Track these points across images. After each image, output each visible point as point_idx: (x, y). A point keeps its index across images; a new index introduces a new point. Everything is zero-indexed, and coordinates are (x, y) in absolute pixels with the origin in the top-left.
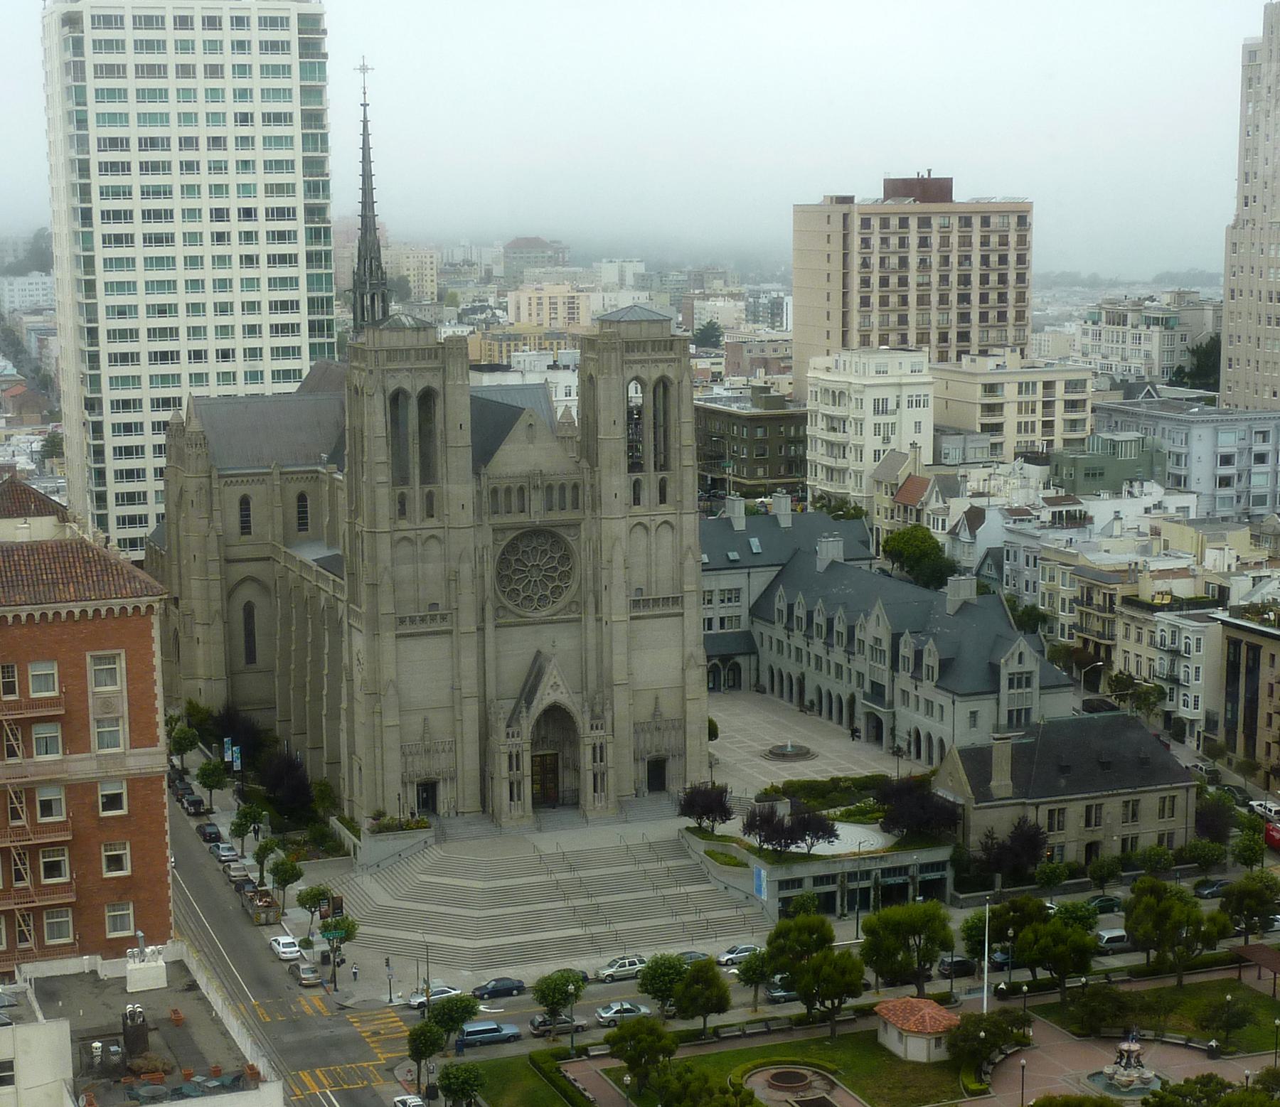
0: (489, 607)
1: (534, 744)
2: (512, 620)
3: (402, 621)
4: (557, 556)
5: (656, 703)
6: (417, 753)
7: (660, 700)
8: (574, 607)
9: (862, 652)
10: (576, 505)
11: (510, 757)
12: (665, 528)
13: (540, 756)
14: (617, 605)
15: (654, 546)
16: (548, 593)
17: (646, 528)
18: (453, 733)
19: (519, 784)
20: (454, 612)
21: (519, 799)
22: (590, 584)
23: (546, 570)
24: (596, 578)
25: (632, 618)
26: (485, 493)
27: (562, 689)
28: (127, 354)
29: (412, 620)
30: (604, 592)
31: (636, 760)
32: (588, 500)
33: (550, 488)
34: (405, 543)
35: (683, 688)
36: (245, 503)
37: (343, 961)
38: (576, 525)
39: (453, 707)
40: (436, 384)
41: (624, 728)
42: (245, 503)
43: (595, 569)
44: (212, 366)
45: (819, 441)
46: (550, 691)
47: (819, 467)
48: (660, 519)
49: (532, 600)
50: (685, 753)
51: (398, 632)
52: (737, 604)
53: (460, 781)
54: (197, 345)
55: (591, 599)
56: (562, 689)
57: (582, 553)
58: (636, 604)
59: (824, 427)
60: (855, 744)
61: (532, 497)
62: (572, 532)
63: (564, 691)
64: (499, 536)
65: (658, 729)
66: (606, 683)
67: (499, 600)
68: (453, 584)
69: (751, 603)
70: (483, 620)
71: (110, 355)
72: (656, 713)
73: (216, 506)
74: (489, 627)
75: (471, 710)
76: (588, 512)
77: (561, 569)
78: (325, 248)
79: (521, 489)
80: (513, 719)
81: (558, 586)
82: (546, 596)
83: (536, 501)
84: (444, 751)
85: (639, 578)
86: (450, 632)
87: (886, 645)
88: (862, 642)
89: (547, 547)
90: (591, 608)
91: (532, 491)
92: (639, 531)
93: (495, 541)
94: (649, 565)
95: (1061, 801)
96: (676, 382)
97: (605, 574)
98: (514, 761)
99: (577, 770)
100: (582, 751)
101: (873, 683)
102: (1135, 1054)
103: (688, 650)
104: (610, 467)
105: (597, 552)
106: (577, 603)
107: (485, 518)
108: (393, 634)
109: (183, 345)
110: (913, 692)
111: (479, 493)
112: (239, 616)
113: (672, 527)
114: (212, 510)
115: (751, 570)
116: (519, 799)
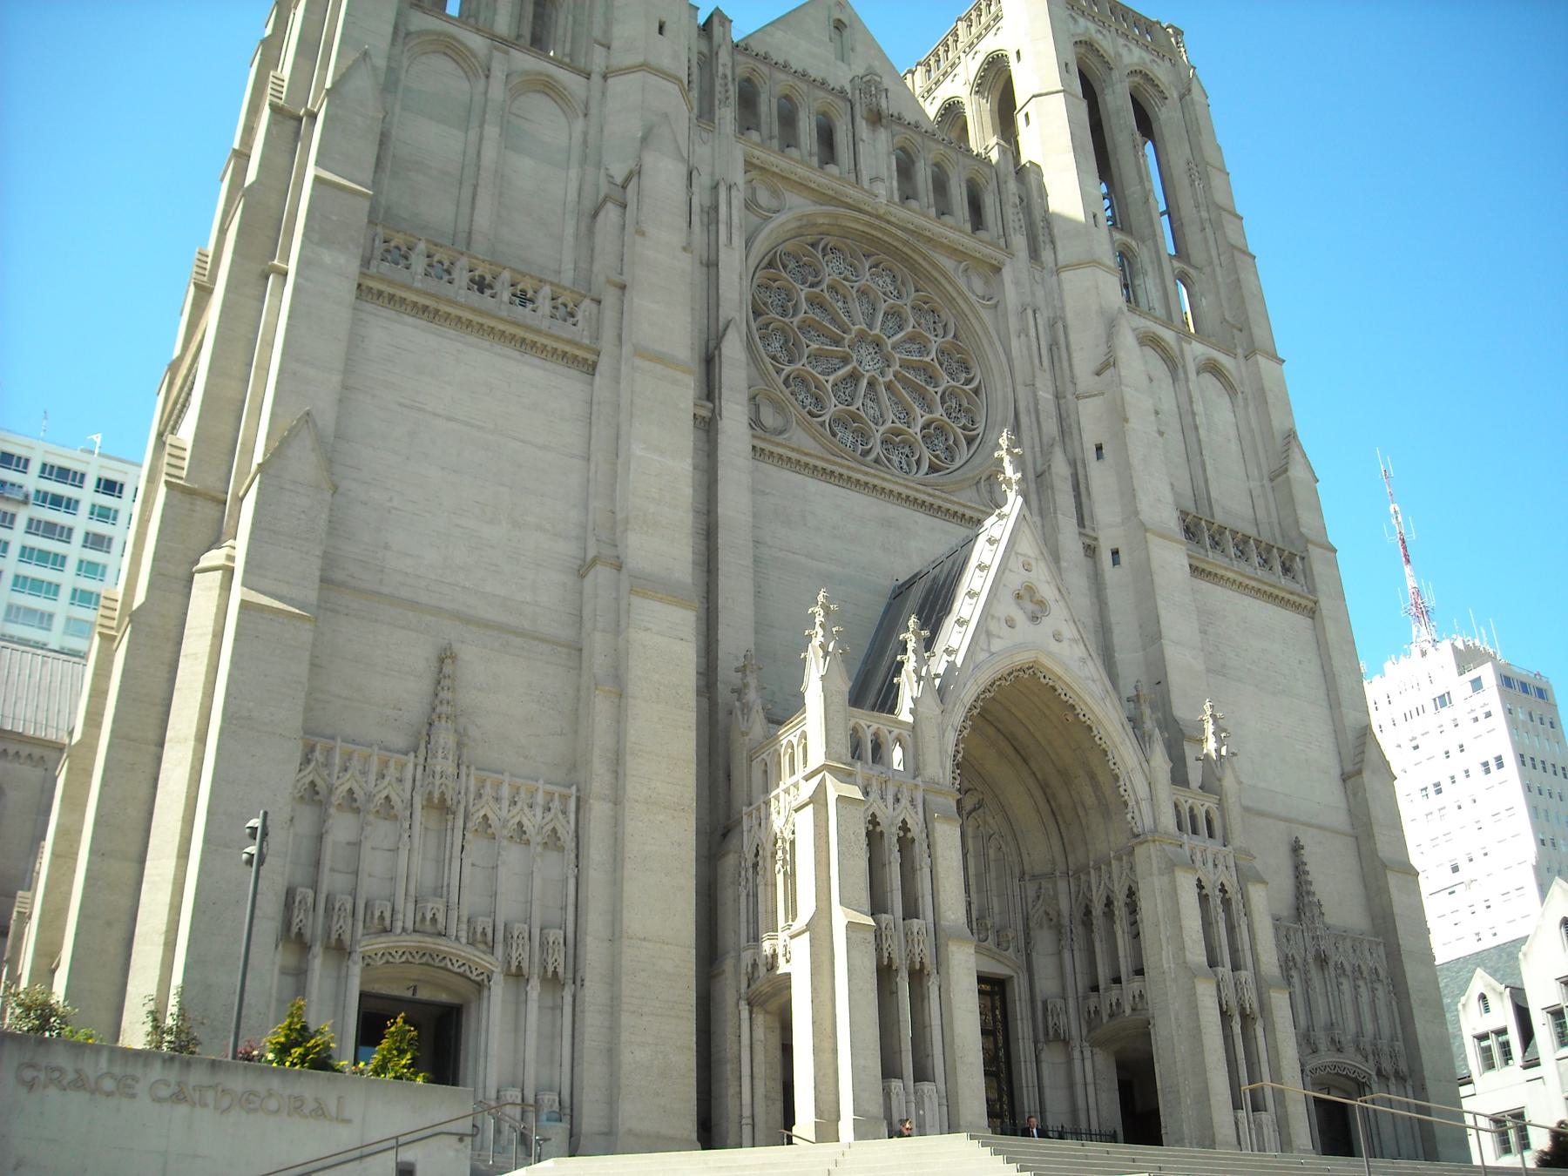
0: (733, 350)
7: (1307, 855)
15: (1198, 407)
17: (1172, 363)
20: (610, 298)
22: (1051, 427)
23: (905, 365)
27: (1057, 617)
39: (577, 650)
43: (1058, 396)
46: (1020, 617)
49: (863, 435)
53: (594, 992)
56: (1057, 617)
57: (1015, 343)
63: (1068, 631)
65: (1322, 960)
68: (611, 213)
76: (1019, 242)
77: (945, 381)
81: (940, 429)
91: (863, 128)
93: (750, 204)
113: (1229, 387)
116: (921, 1075)
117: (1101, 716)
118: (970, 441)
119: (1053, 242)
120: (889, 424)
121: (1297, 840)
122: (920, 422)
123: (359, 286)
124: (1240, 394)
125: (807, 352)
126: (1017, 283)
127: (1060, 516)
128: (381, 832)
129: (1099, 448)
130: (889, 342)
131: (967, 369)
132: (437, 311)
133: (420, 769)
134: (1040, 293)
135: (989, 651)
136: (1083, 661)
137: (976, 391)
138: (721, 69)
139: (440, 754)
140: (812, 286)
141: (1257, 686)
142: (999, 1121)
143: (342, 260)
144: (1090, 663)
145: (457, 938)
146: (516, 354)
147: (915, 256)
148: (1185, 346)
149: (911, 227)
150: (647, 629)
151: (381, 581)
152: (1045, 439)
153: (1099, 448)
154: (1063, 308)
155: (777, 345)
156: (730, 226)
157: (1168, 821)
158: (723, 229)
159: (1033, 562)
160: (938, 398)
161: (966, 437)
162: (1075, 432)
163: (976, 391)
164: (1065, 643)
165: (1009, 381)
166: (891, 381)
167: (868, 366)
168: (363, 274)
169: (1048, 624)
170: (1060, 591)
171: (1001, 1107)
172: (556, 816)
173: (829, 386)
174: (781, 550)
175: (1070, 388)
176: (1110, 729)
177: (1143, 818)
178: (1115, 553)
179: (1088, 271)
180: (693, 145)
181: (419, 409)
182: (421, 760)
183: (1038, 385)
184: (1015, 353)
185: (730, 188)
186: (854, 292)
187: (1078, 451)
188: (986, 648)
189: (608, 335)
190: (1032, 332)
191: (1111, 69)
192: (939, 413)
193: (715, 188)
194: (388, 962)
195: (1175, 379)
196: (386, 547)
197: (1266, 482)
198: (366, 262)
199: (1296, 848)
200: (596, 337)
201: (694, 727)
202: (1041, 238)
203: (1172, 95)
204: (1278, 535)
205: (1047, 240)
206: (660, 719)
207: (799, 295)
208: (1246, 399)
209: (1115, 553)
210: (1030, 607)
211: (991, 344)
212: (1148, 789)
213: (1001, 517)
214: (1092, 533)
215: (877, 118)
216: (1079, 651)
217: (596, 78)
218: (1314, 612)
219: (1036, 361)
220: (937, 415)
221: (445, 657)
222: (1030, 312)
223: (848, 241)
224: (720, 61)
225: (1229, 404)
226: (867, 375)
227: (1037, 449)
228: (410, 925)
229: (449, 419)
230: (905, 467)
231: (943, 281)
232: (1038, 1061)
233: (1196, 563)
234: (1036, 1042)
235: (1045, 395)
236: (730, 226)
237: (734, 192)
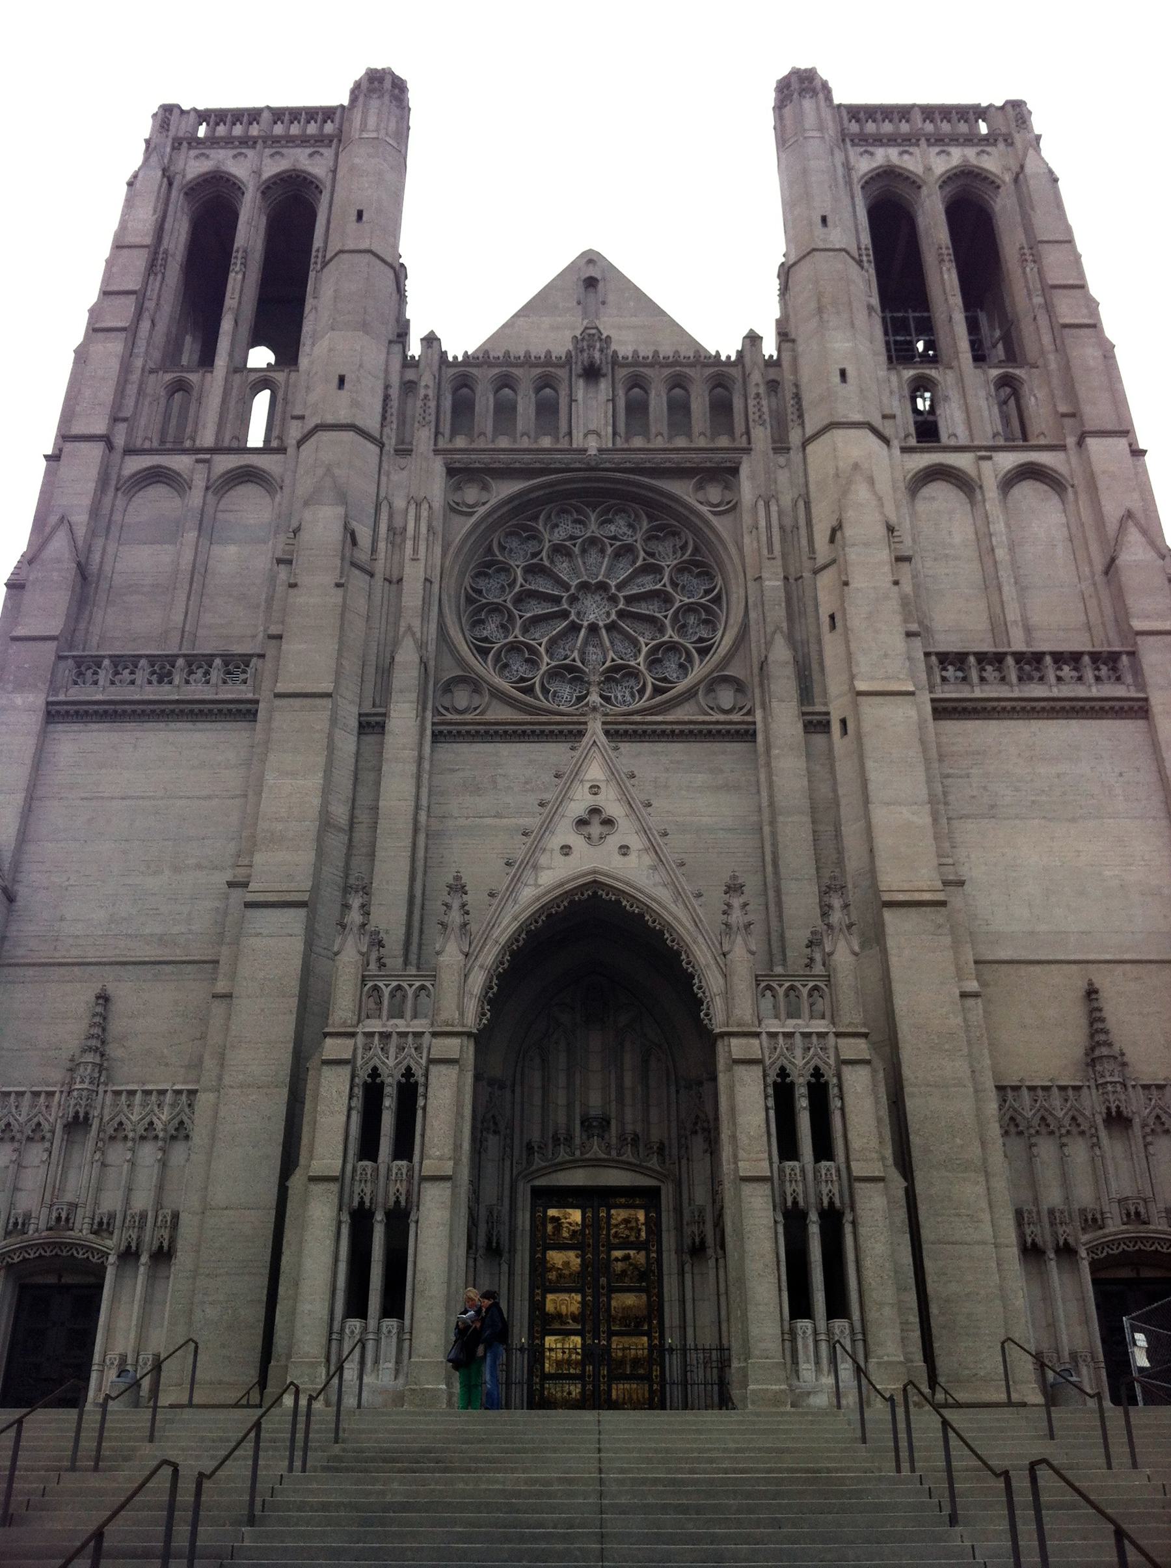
0: (407, 656)
2: (500, 713)
3: (86, 666)
4: (669, 562)
6: (36, 1134)
8: (726, 697)
11: (372, 1092)
12: (1027, 491)
18: (197, 1064)
22: (777, 614)
23: (629, 600)
25: (943, 710)
27: (626, 832)
29: (123, 663)
30: (827, 637)
31: (1031, 1252)
33: (637, 382)
34: (157, 493)
38: (726, 474)
40: (317, 167)
48: (1008, 461)
51: (62, 697)
55: (781, 653)
56: (626, 832)
57: (747, 540)
61: (580, 394)
62: (714, 493)
63: (636, 842)
64: (471, 494)
65: (1118, 1120)
67: (461, 662)
76: (761, 436)
81: (672, 647)
82: (634, 674)
84: (148, 1133)
86: (245, 712)
89: (637, 539)
90: (783, 684)
93: (453, 509)
94: (991, 585)
96: (1008, 178)
104: (820, 310)
106: (739, 686)
108: (36, 699)
117: (670, 919)
118: (703, 652)
119: (801, 416)
120: (608, 664)
121: (1091, 984)
122: (645, 650)
123: (48, 713)
124: (1070, 490)
125: (519, 622)
126: (752, 477)
127: (774, 704)
128: (36, 1154)
129: (832, 617)
130: (613, 583)
131: (712, 578)
132: (115, 712)
133: (65, 1094)
134: (783, 477)
135: (537, 886)
136: (654, 868)
137: (717, 600)
138: (422, 392)
139: (78, 1080)
140: (534, 555)
141: (1044, 818)
142: (645, 1339)
143: (31, 698)
144: (661, 868)
145: (81, 1231)
146: (189, 725)
147: (643, 492)
148: (981, 462)
149: (628, 465)
150: (258, 935)
151: (55, 949)
152: (769, 629)
153: (832, 617)
154: (807, 485)
155: (493, 626)
156: (416, 538)
158: (409, 544)
159: (603, 785)
160: (667, 622)
161: (699, 651)
162: (810, 610)
164: (633, 857)
165: (741, 580)
166: (613, 621)
167: (594, 611)
168: (48, 703)
169: (614, 841)
170: (631, 806)
171: (650, 1324)
172: (182, 1110)
173: (542, 650)
174: (467, 818)
175: (807, 564)
176: (681, 930)
178: (844, 722)
179: (828, 435)
180: (388, 475)
181: (97, 798)
182: (66, 1088)
183: (765, 575)
184: (747, 550)
185: (418, 505)
186: (576, 550)
187: (812, 629)
188: (531, 882)
189: (266, 685)
190: (762, 523)
191: (919, 187)
192: (670, 635)
194: (56, 1254)
195: (972, 503)
196: (62, 919)
197: (1099, 578)
198: (53, 688)
199: (1091, 993)
201: (295, 1010)
202: (790, 417)
203: (1004, 182)
204: (1112, 634)
205: (795, 417)
206: (262, 1010)
207: (516, 573)
208: (1076, 493)
209: (844, 722)
210: (595, 829)
211: (726, 549)
212: (721, 981)
213: (573, 749)
214: (823, 709)
215: (592, 373)
216: (648, 860)
217: (291, 451)
218: (1147, 711)
219: (765, 552)
220: (666, 638)
221: (104, 998)
222: (761, 503)
223: (573, 502)
224: (423, 384)
225: (1060, 506)
226: (585, 624)
227: (763, 641)
228: (42, 1226)
229: (123, 798)
230: (628, 698)
231: (673, 505)
232: (682, 1273)
233: (937, 704)
234: (679, 1251)
235: (773, 583)
236: (416, 538)
237: (425, 506)
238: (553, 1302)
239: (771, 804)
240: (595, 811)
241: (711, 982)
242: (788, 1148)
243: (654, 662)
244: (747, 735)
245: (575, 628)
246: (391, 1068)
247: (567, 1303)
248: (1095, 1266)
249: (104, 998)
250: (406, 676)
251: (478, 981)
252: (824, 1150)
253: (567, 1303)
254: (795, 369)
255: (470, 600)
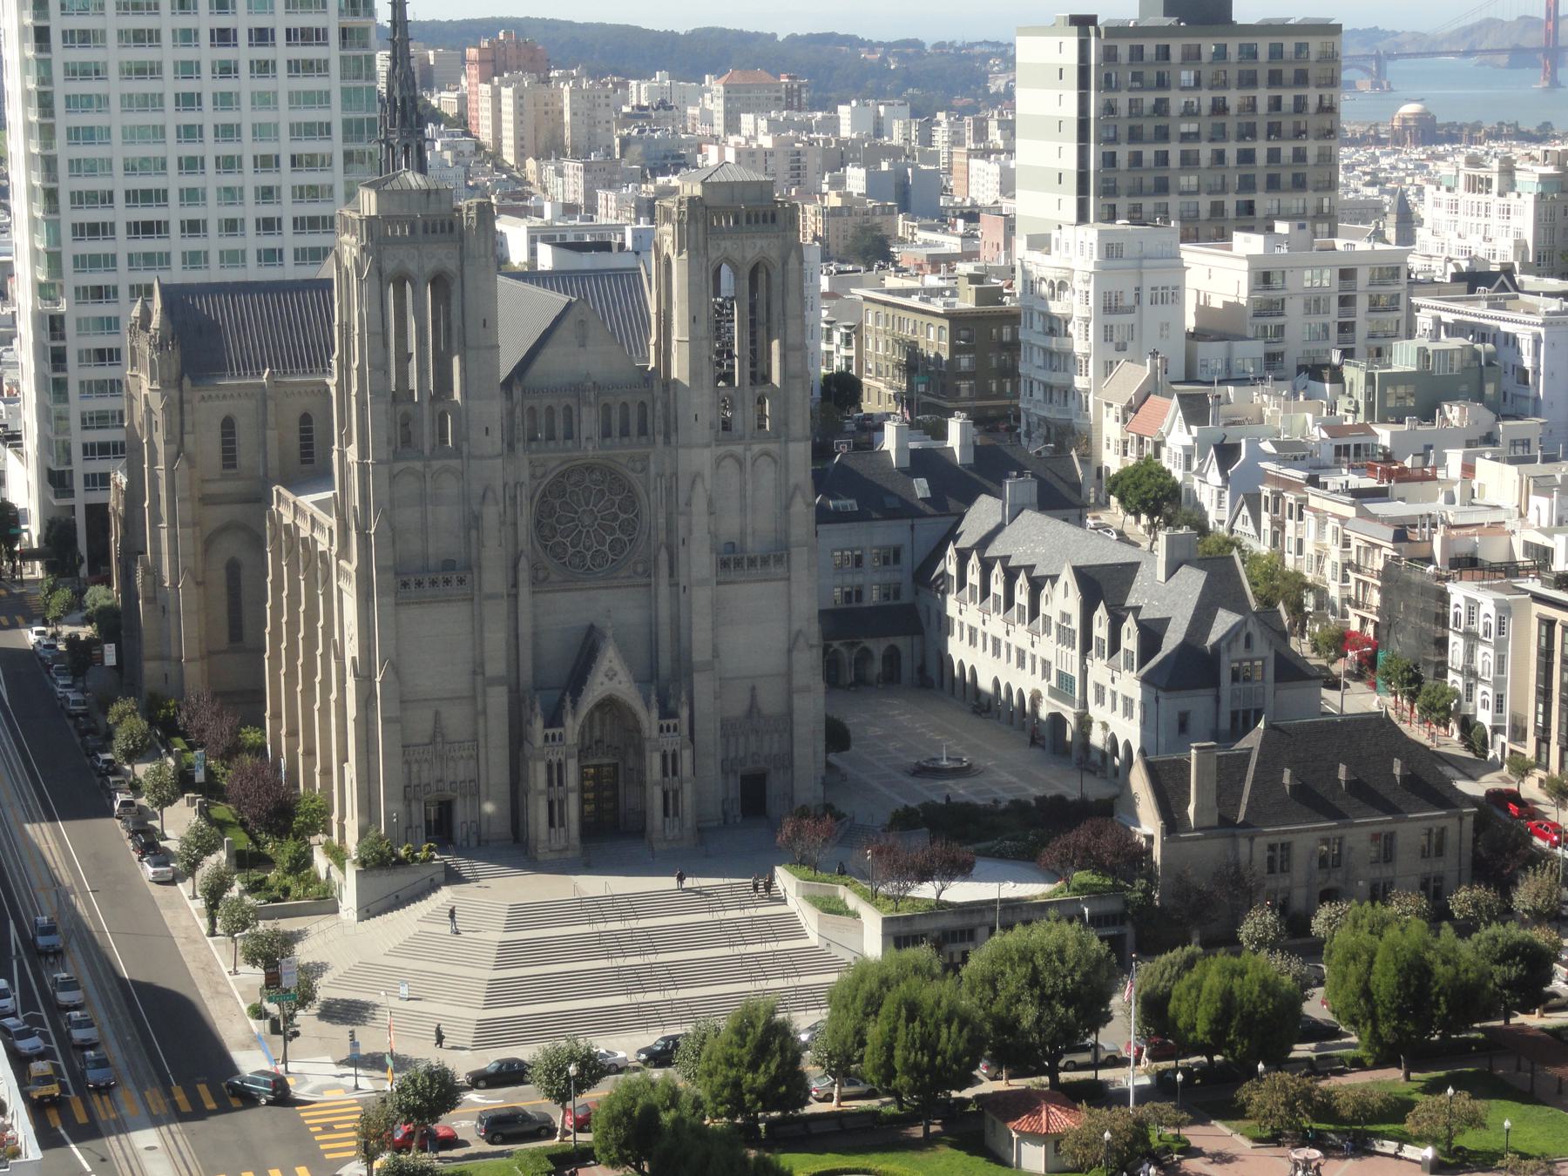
0: (523, 564)
1: (584, 752)
4: (617, 499)
5: (753, 697)
9: (1047, 631)
10: (643, 431)
13: (595, 766)
14: (699, 560)
15: (749, 487)
16: (606, 548)
17: (740, 463)
19: (561, 803)
21: (562, 825)
22: (662, 536)
24: (670, 529)
25: (718, 583)
26: (518, 411)
28: (97, 224)
30: (681, 547)
32: (660, 425)
35: (789, 674)
36: (228, 426)
37: (296, 1034)
39: (474, 698)
40: (452, 265)
41: (708, 731)
42: (228, 426)
44: (214, 243)
45: (1035, 349)
46: (606, 680)
47: (1035, 385)
48: (757, 448)
49: (584, 557)
50: (792, 764)
52: (896, 567)
54: (194, 213)
55: (663, 556)
57: (651, 496)
58: (724, 564)
59: (1041, 329)
60: (1036, 752)
61: (584, 417)
63: (624, 679)
66: (684, 668)
68: (474, 533)
69: (916, 567)
70: (515, 585)
71: (74, 225)
72: (753, 709)
73: (188, 428)
74: (524, 591)
75: (498, 699)
76: (660, 439)
77: (623, 516)
78: (367, 84)
79: (568, 408)
80: (554, 719)
83: (589, 421)
85: (730, 526)
87: (1075, 624)
88: (1047, 619)
92: (729, 463)
95: (1285, 832)
97: (682, 521)
98: (555, 773)
99: (642, 784)
100: (647, 760)
101: (1061, 675)
102: (1314, 1164)
103: (796, 626)
105: (671, 491)
107: (519, 446)
109: (174, 213)
110: (1109, 687)
111: (511, 413)
112: (219, 575)
113: (776, 462)
114: (182, 434)
115: (916, 521)
137: (636, 516)
157: (655, 733)
163: (636, 516)
169: (616, 679)
177: (647, 735)
192: (618, 534)
193: (516, 486)
199: (753, 689)
200: (473, 588)
210: (611, 674)
221: (437, 713)
235: (662, 521)
238: (586, 796)
239: (656, 617)
240: (611, 669)
241: (645, 723)
242: (665, 773)
243: (611, 548)
244: (649, 585)
245: (580, 532)
246: (555, 759)
247: (591, 796)
248: (742, 777)
249: (437, 713)
250: (524, 576)
251: (578, 728)
252: (675, 773)
253: (591, 796)
254: (676, 403)
255: (539, 522)
